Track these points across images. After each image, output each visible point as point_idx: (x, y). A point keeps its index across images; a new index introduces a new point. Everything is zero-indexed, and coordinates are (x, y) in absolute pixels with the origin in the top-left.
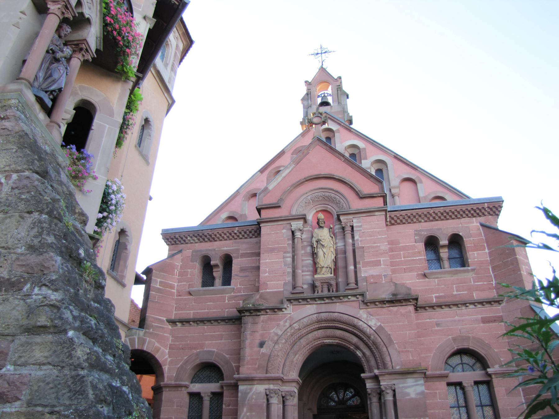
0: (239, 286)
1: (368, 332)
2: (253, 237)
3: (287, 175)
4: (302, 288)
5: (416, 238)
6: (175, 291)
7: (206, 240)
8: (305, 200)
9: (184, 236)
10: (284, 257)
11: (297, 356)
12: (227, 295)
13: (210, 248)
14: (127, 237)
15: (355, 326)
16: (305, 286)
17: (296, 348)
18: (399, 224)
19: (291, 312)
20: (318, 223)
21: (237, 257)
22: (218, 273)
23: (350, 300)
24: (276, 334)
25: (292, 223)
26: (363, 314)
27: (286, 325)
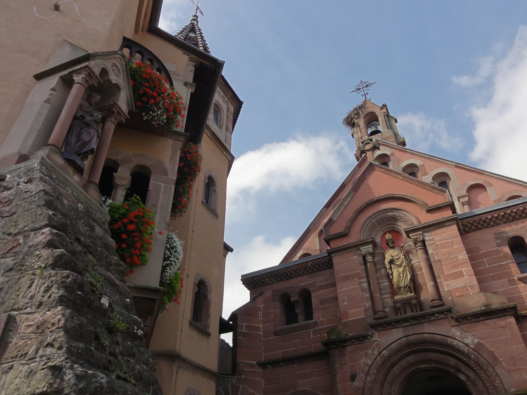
0: (321, 319)
1: (467, 352)
2: (327, 268)
3: (348, 204)
4: (384, 312)
5: (497, 242)
6: (261, 333)
7: (283, 278)
8: (370, 224)
9: (262, 278)
10: (360, 283)
11: (393, 387)
12: (311, 330)
13: (288, 286)
14: (206, 288)
15: (450, 346)
16: (387, 310)
17: (389, 378)
18: (474, 230)
19: (377, 339)
20: (388, 244)
22: (299, 310)
23: (438, 318)
24: (366, 364)
25: (361, 248)
26: (456, 332)
27: (375, 354)
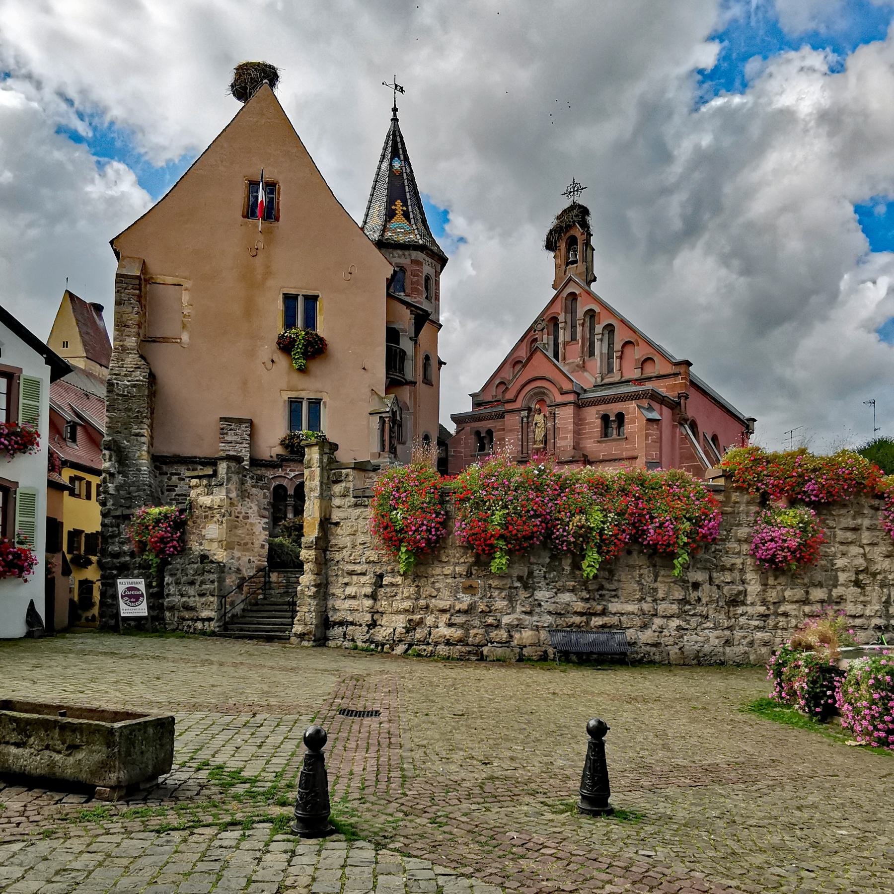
21: (496, 432)
